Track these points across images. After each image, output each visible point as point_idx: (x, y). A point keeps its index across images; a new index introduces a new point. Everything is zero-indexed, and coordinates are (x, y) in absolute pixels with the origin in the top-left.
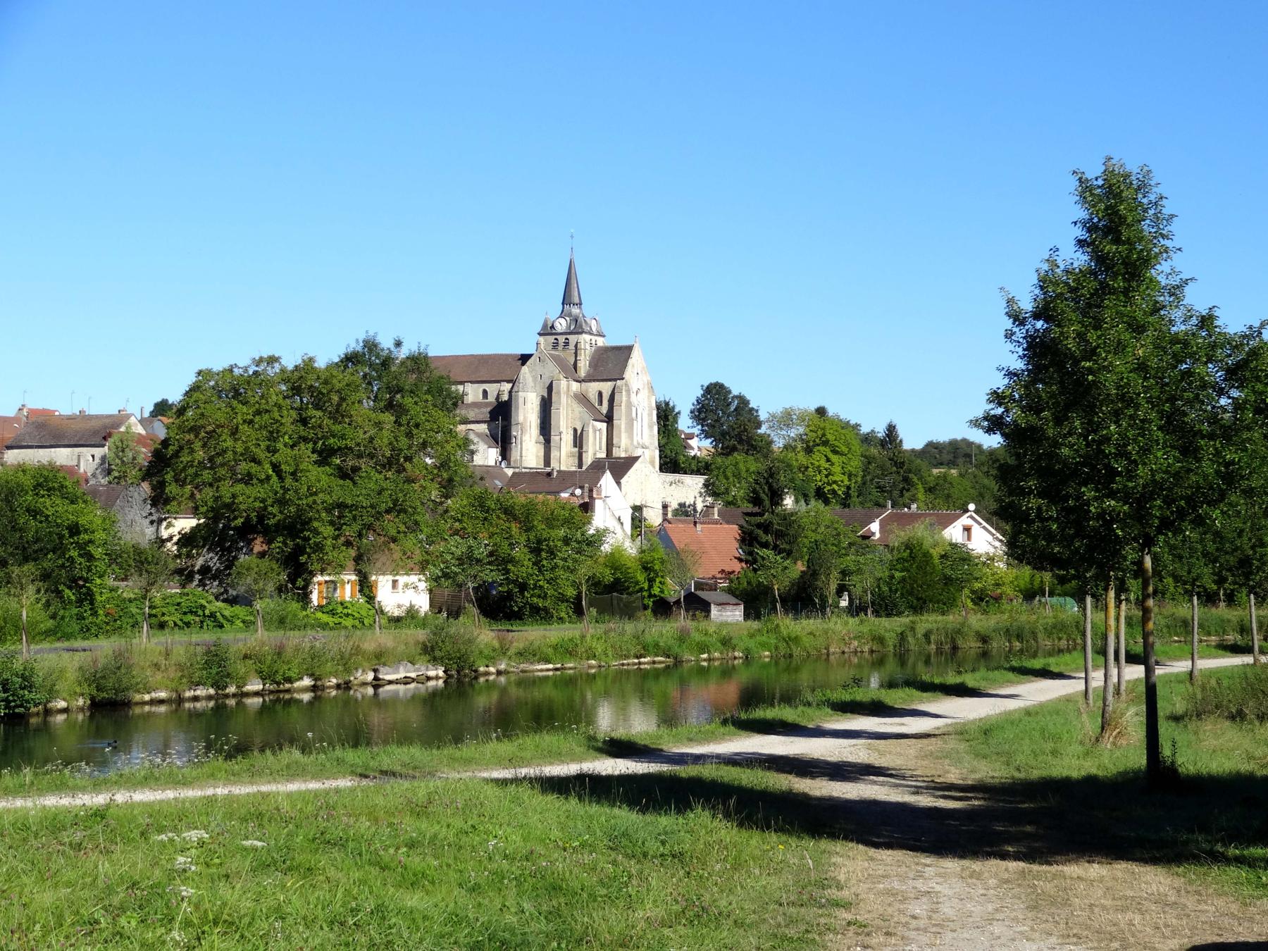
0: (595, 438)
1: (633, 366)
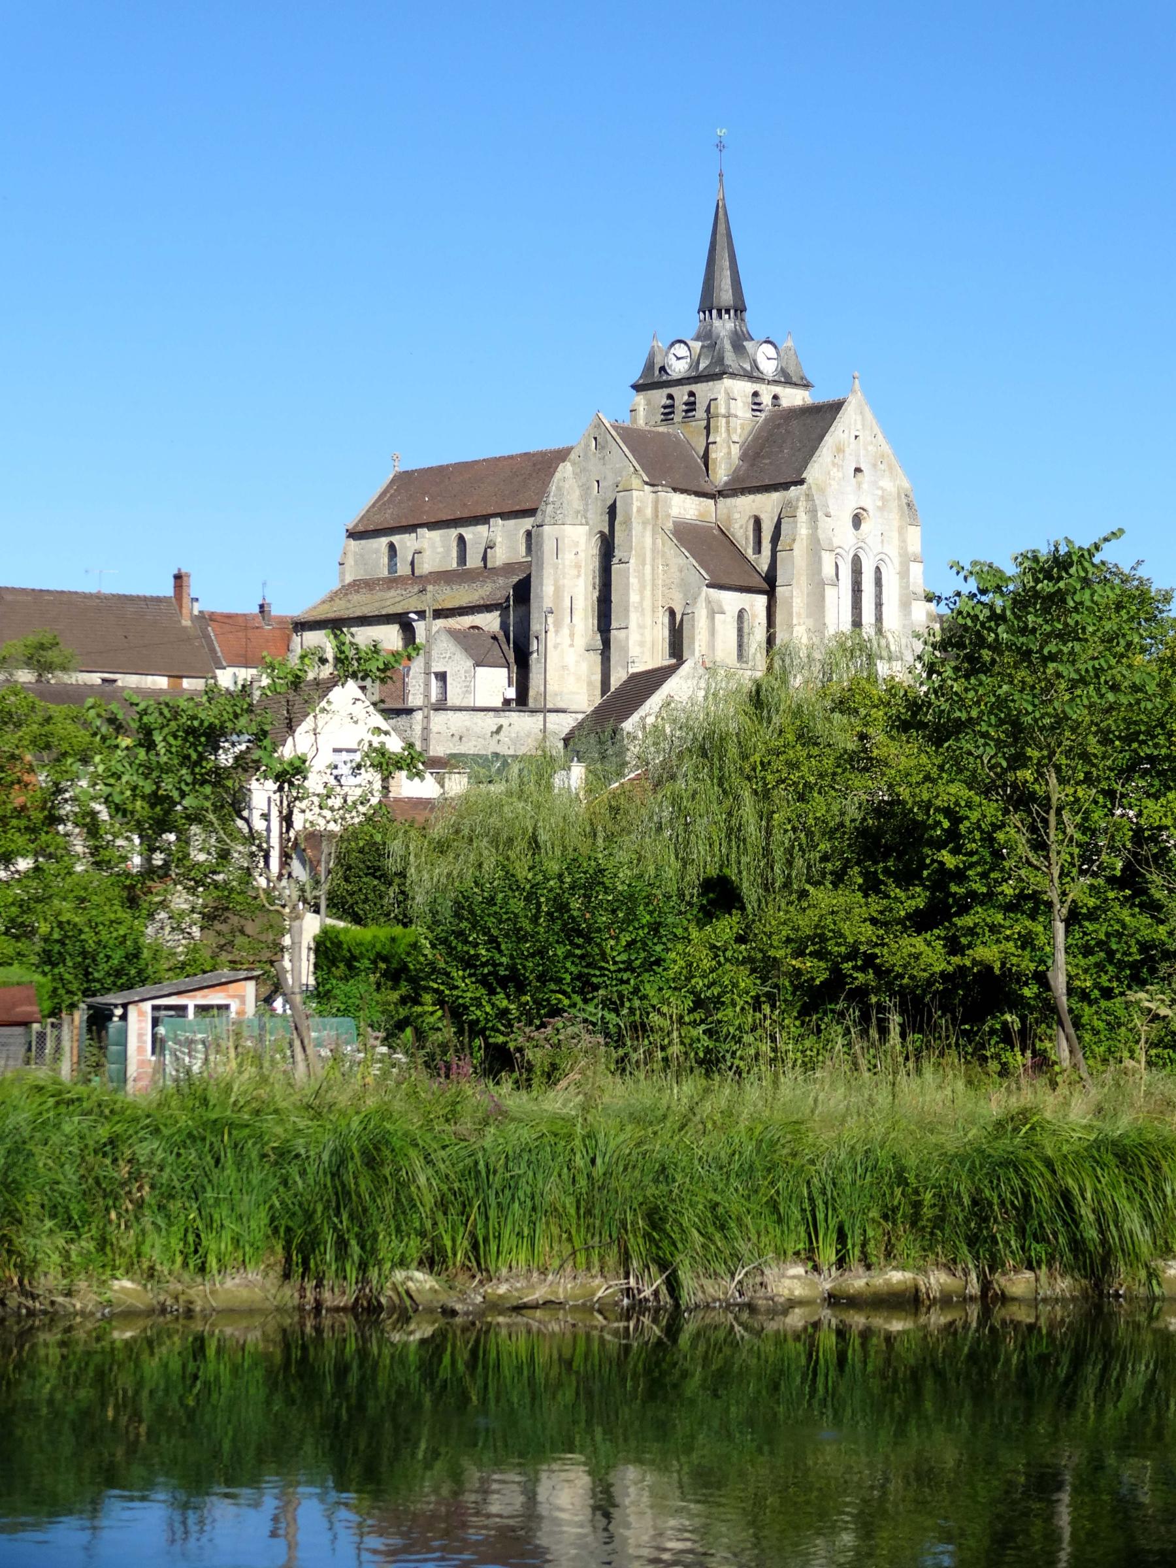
0: (712, 632)
1: (840, 450)
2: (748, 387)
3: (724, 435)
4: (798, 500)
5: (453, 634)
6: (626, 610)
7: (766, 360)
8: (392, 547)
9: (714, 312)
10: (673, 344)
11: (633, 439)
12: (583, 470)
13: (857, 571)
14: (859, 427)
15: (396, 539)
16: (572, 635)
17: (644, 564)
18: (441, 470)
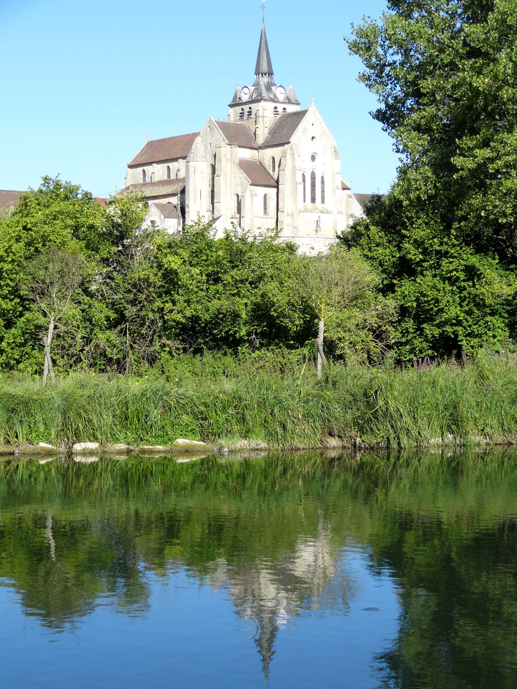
3: (262, 124)
4: (287, 150)
5: (156, 205)
6: (220, 195)
7: (280, 93)
8: (144, 171)
9: (260, 75)
10: (243, 88)
11: (225, 127)
12: (205, 139)
13: (313, 178)
15: (145, 168)
17: (227, 177)
18: (164, 140)
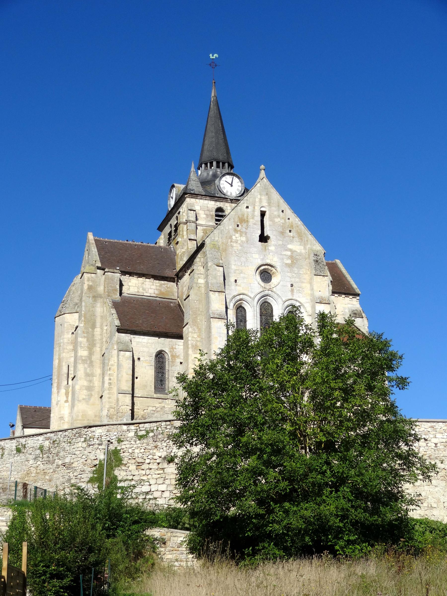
2: (213, 205)
14: (265, 203)
16: (67, 394)
17: (94, 327)
